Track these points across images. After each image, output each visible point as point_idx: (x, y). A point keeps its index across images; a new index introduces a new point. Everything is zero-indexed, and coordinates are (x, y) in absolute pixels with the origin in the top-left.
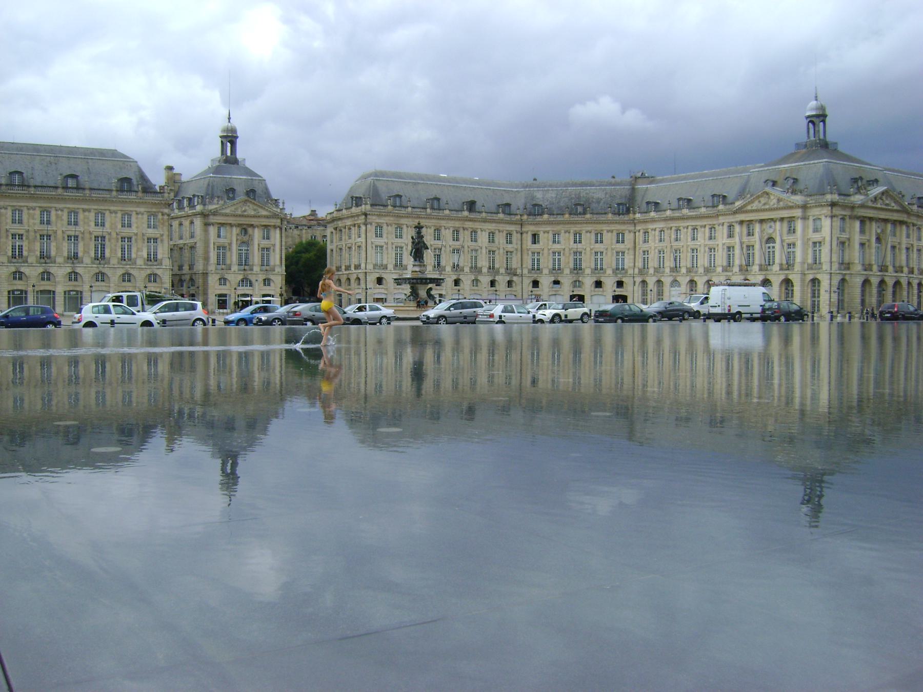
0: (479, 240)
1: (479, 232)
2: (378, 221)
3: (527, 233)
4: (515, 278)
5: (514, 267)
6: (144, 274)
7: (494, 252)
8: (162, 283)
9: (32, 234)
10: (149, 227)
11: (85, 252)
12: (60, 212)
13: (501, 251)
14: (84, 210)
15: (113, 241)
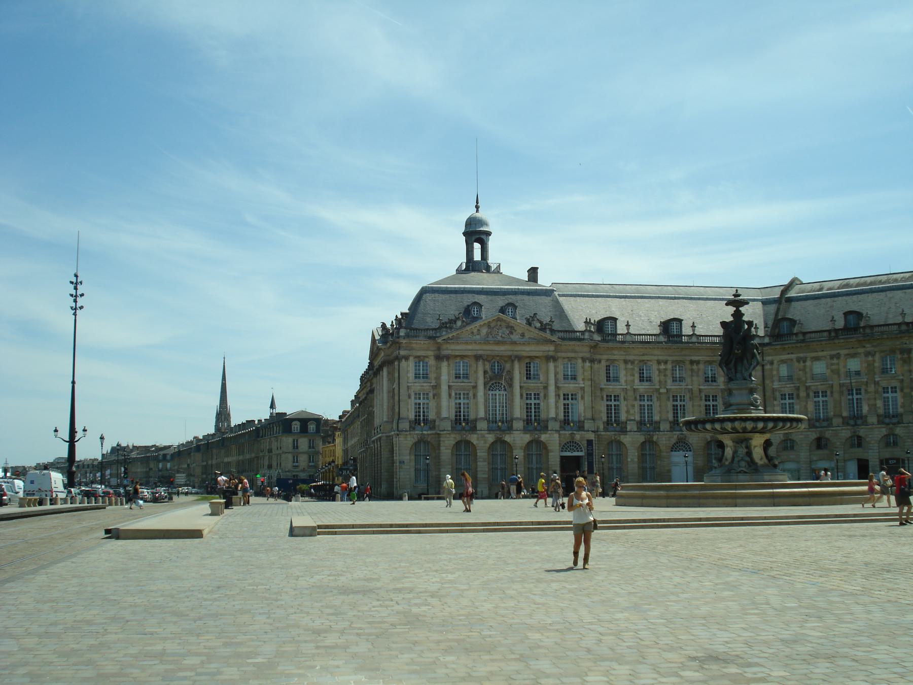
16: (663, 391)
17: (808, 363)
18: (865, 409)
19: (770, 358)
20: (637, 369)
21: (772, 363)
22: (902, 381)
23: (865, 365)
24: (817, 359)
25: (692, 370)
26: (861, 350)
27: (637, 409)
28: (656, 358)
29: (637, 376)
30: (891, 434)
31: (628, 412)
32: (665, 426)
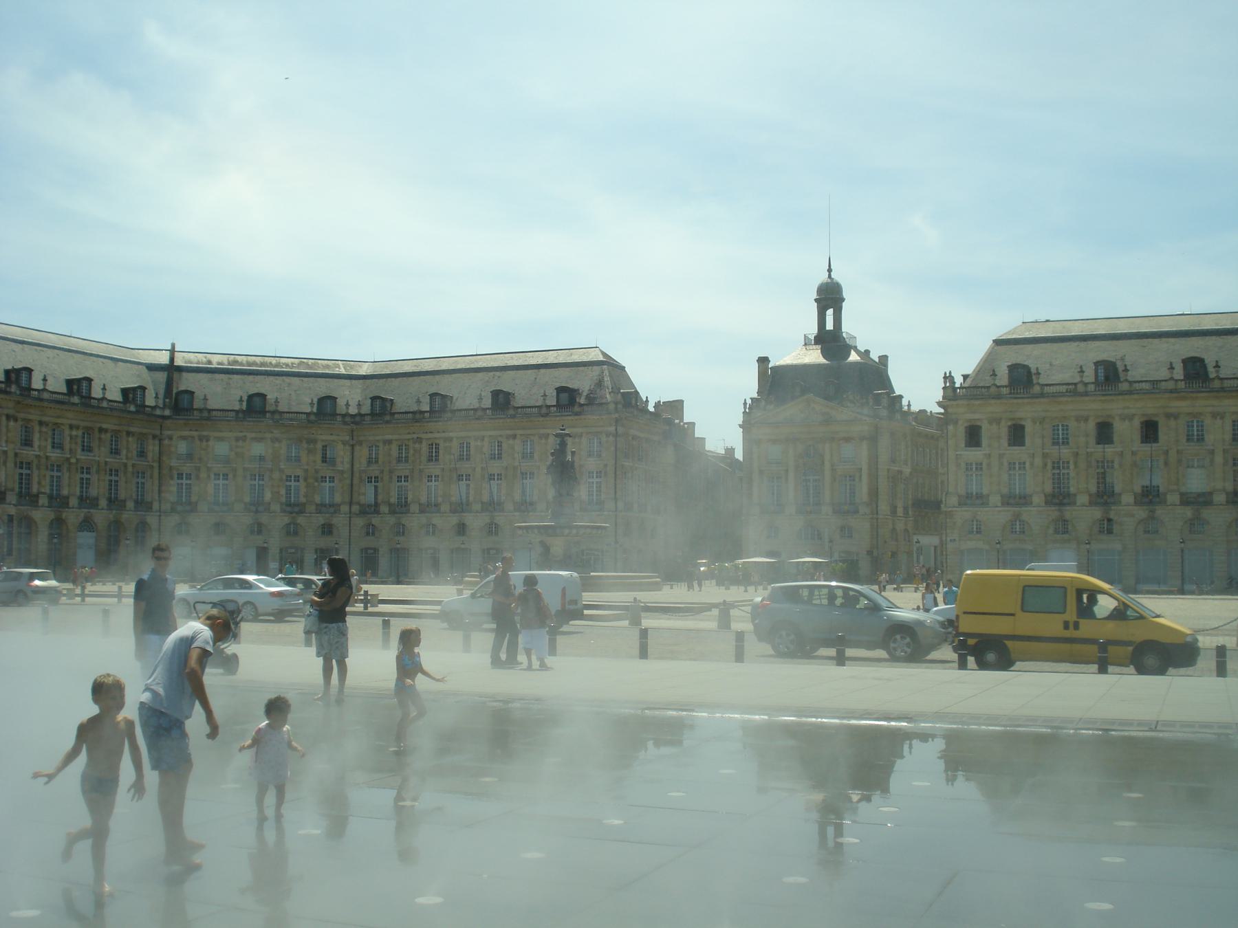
0: (1209, 438)
1: (1208, 421)
2: (969, 416)
12: (479, 443)
14: (508, 437)
16: (73, 460)
17: (211, 443)
18: (268, 496)
19: (169, 433)
20: (50, 433)
21: (170, 438)
22: (306, 471)
24: (221, 439)
25: (100, 439)
26: (268, 435)
27: (48, 479)
28: (69, 422)
29: (50, 440)
30: (369, 525)
31: (39, 483)
32: (74, 502)
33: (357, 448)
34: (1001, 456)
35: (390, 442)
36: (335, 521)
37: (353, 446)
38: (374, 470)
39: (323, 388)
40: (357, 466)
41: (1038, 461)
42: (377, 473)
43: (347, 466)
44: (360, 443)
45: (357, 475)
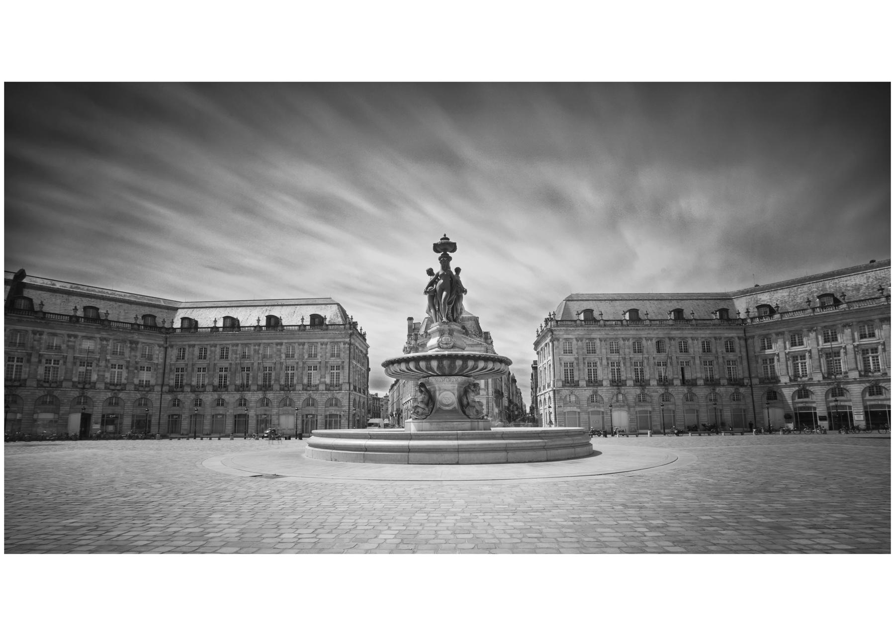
0: (691, 350)
1: (690, 341)
2: (565, 336)
3: (753, 337)
4: (742, 390)
5: (741, 376)
6: (325, 398)
7: (711, 363)
8: (342, 406)
9: (234, 366)
10: (332, 355)
11: (276, 380)
13: (721, 360)
14: (277, 344)
15: (299, 369)
23: (99, 346)
33: (169, 349)
34: (584, 359)
35: (194, 346)
36: (149, 396)
37: (166, 348)
38: (181, 364)
39: (147, 311)
40: (168, 361)
41: (605, 362)
42: (183, 366)
43: (161, 361)
44: (172, 346)
45: (168, 367)
